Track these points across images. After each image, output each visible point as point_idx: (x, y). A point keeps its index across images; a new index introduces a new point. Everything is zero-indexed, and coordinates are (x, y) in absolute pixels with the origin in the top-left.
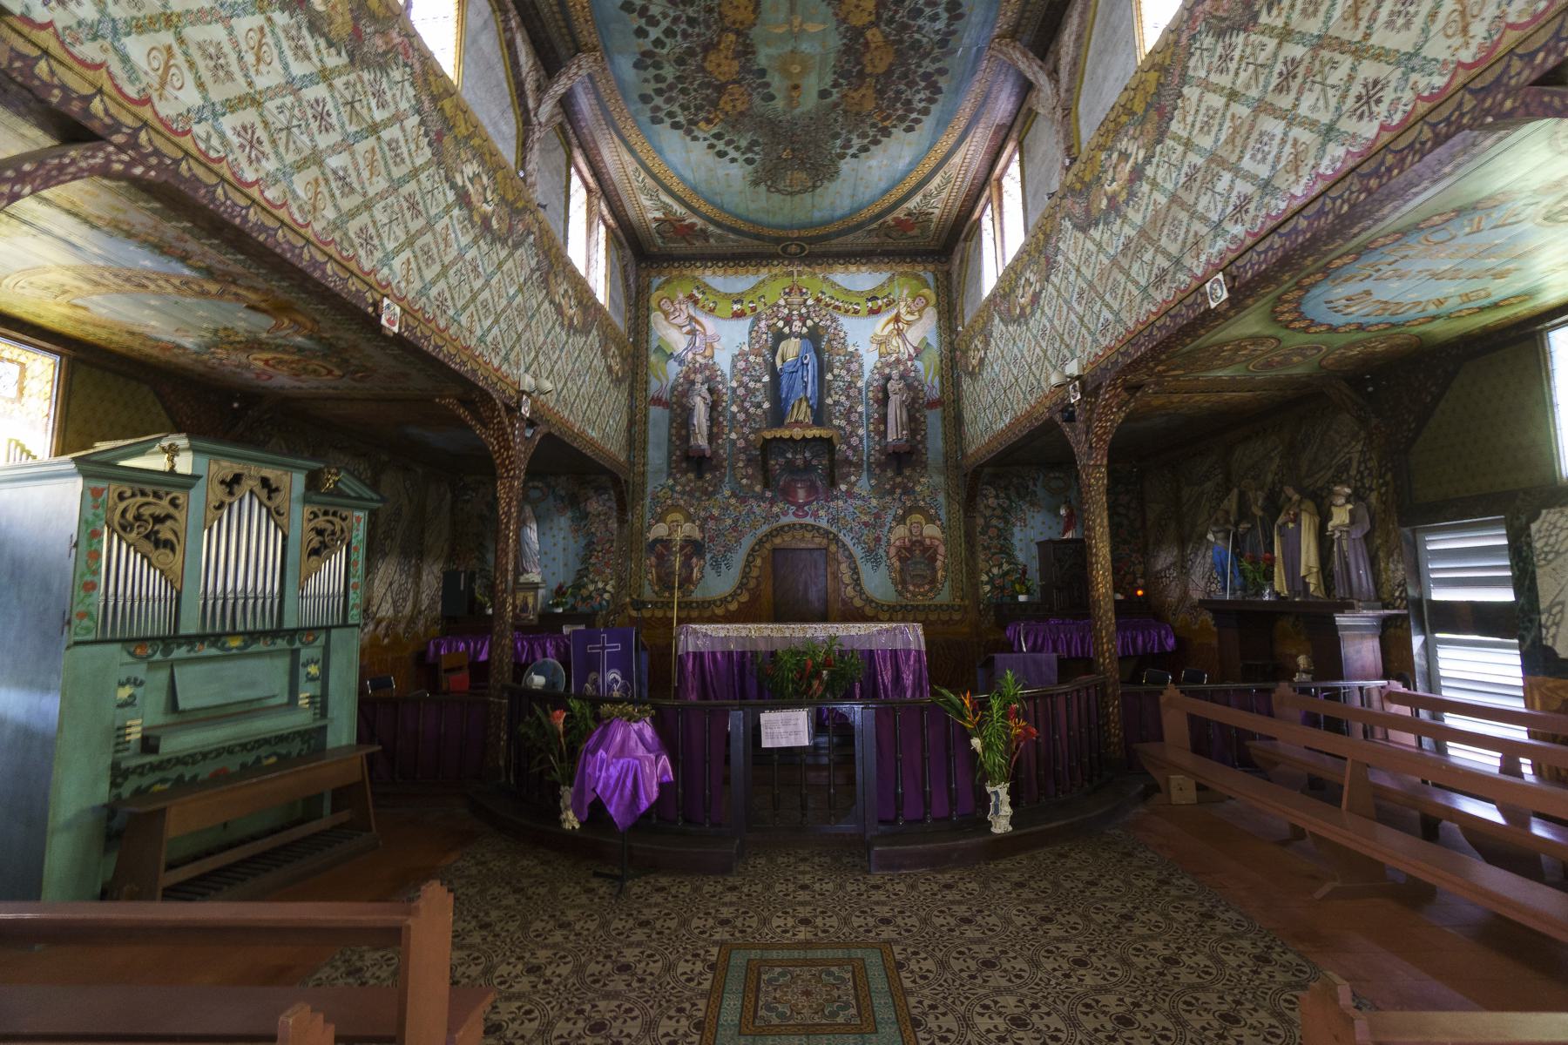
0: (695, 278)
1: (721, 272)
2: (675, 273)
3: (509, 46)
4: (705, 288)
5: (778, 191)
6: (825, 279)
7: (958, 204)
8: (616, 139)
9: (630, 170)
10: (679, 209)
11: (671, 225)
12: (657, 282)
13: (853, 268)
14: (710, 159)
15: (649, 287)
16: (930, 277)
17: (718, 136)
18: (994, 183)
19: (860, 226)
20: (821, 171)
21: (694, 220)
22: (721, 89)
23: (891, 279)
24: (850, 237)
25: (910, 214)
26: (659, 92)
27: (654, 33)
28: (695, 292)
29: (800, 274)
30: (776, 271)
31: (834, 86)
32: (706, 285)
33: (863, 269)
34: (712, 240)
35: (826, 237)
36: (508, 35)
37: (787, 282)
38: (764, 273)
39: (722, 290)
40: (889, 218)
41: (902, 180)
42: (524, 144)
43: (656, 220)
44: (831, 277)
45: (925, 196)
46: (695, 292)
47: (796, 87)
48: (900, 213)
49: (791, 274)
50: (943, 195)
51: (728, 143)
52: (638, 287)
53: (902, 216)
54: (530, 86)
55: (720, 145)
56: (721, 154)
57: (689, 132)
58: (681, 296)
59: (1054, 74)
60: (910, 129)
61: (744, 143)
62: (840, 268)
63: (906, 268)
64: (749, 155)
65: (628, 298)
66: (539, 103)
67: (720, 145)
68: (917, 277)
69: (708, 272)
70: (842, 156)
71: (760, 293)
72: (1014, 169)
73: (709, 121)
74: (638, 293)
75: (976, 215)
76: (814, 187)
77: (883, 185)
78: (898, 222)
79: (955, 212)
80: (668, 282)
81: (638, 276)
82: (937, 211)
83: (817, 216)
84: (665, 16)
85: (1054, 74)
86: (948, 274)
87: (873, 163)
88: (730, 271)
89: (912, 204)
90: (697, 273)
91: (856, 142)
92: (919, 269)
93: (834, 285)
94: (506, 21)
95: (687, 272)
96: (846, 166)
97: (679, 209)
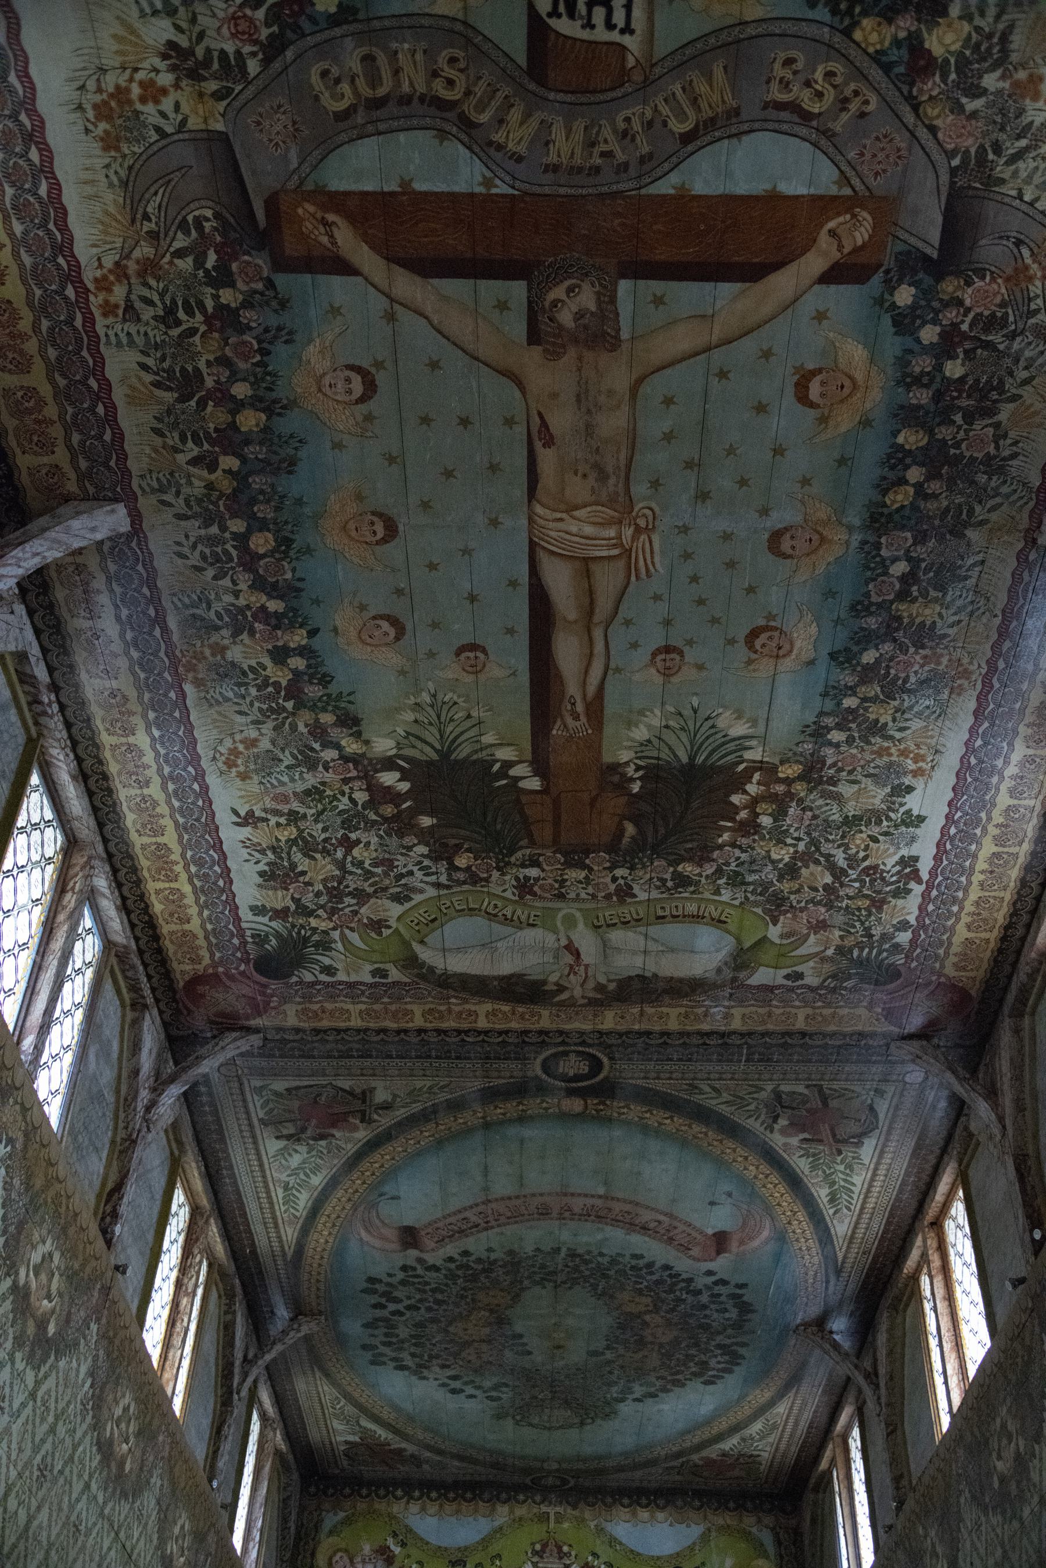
0: (392, 1517)
1: (433, 1508)
2: (361, 1506)
3: (226, 1328)
4: (407, 1537)
5: (531, 1425)
6: (600, 1530)
7: (794, 1449)
8: (318, 1374)
9: (327, 1400)
10: (382, 1434)
11: (368, 1449)
12: (330, 1520)
13: (644, 1514)
14: (440, 1395)
15: (317, 1528)
16: (767, 1538)
17: (455, 1378)
18: (838, 1440)
19: (652, 1463)
20: (588, 1409)
21: (403, 1445)
22: (467, 1344)
23: (705, 1538)
24: (638, 1474)
25: (724, 1454)
26: (384, 1344)
27: (392, 1307)
28: (390, 1542)
29: (559, 1518)
30: (521, 1511)
31: (608, 1348)
32: (409, 1530)
33: (660, 1515)
34: (426, 1467)
35: (601, 1472)
36: (229, 1317)
37: (537, 1532)
38: (503, 1510)
39: (433, 1540)
40: (695, 1457)
41: (708, 1422)
42: (219, 1431)
43: (346, 1442)
44: (609, 1527)
45: (743, 1440)
46: (390, 1542)
47: (559, 1347)
48: (712, 1452)
49: (544, 1518)
50: (770, 1440)
51: (466, 1383)
52: (299, 1527)
53: (714, 1456)
54: (239, 1355)
55: (457, 1384)
56: (454, 1391)
57: (415, 1373)
58: (367, 1549)
59: (872, 1376)
60: (707, 1383)
61: (487, 1384)
62: (623, 1513)
63: (726, 1519)
64: (494, 1394)
65: (281, 1548)
66: (245, 1375)
67: (457, 1384)
68: (746, 1536)
69: (414, 1507)
70: (623, 1400)
71: (495, 1548)
72: (856, 1433)
73: (443, 1367)
74: (298, 1538)
75: (824, 1465)
76: (582, 1424)
77: (680, 1426)
78: (709, 1463)
79: (791, 1459)
80: (348, 1521)
81: (302, 1508)
82: (765, 1455)
83: (588, 1450)
84: (409, 1298)
85: (872, 1376)
86: (797, 1533)
87: (666, 1407)
88: (448, 1508)
89: (727, 1445)
90: (396, 1508)
91: (638, 1390)
92: (749, 1521)
93: (612, 1541)
94: (230, 1305)
95: (380, 1506)
96: (626, 1408)
97: (382, 1434)
